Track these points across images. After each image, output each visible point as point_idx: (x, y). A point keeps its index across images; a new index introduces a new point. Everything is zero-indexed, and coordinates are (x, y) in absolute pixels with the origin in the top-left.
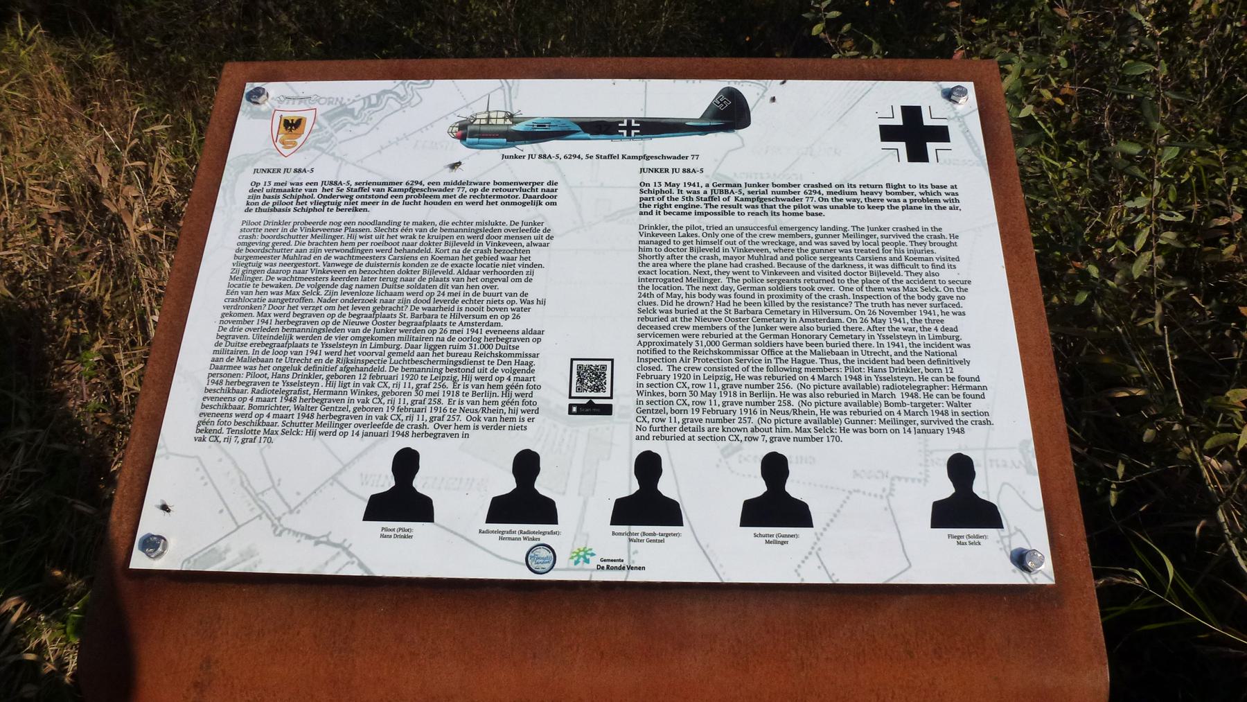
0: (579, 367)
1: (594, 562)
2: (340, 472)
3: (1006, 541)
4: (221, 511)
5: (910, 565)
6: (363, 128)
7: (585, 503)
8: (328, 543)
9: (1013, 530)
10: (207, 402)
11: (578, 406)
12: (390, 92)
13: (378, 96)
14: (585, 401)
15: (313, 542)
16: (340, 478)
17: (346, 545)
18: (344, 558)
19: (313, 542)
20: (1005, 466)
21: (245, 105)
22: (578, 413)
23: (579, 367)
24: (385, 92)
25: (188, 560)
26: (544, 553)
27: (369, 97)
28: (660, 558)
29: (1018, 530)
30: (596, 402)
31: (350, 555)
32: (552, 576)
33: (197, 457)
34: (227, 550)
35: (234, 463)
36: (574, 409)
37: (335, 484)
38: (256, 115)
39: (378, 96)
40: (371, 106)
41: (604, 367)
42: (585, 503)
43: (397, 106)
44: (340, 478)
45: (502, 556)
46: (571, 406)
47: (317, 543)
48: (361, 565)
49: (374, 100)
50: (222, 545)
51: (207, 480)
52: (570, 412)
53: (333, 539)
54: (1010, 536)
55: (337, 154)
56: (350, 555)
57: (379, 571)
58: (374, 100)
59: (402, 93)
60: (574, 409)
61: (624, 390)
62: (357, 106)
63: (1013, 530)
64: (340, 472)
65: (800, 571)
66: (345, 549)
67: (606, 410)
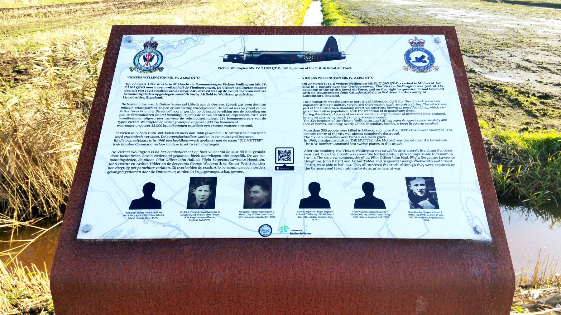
0: (280, 151)
1: (289, 231)
2: (174, 196)
3: (471, 221)
4: (118, 214)
5: (429, 232)
6: (179, 54)
7: (284, 207)
8: (169, 226)
9: (473, 217)
10: (111, 166)
11: (280, 167)
12: (190, 38)
13: (185, 40)
14: (282, 165)
15: (162, 225)
16: (174, 198)
17: (178, 226)
18: (177, 231)
19: (162, 225)
20: (468, 190)
21: (123, 44)
22: (280, 170)
23: (280, 151)
24: (188, 38)
25: (103, 235)
26: (266, 228)
27: (181, 40)
28: (318, 226)
29: (476, 217)
30: (287, 165)
31: (179, 230)
32: (270, 237)
33: (107, 191)
34: (121, 231)
35: (124, 193)
36: (278, 168)
37: (172, 201)
38: (128, 47)
39: (185, 40)
40: (182, 44)
41: (290, 151)
42: (284, 207)
43: (194, 45)
44: (174, 198)
46: (276, 167)
47: (164, 226)
48: (185, 234)
49: (183, 42)
50: (119, 229)
51: (111, 201)
52: (276, 169)
53: (171, 224)
54: (472, 219)
55: (167, 64)
56: (179, 230)
57: (192, 236)
58: (183, 42)
59: (196, 39)
60: (278, 168)
61: (299, 161)
62: (175, 44)
63: (473, 217)
64: (174, 196)
65: (379, 233)
66: (177, 228)
67: (292, 168)
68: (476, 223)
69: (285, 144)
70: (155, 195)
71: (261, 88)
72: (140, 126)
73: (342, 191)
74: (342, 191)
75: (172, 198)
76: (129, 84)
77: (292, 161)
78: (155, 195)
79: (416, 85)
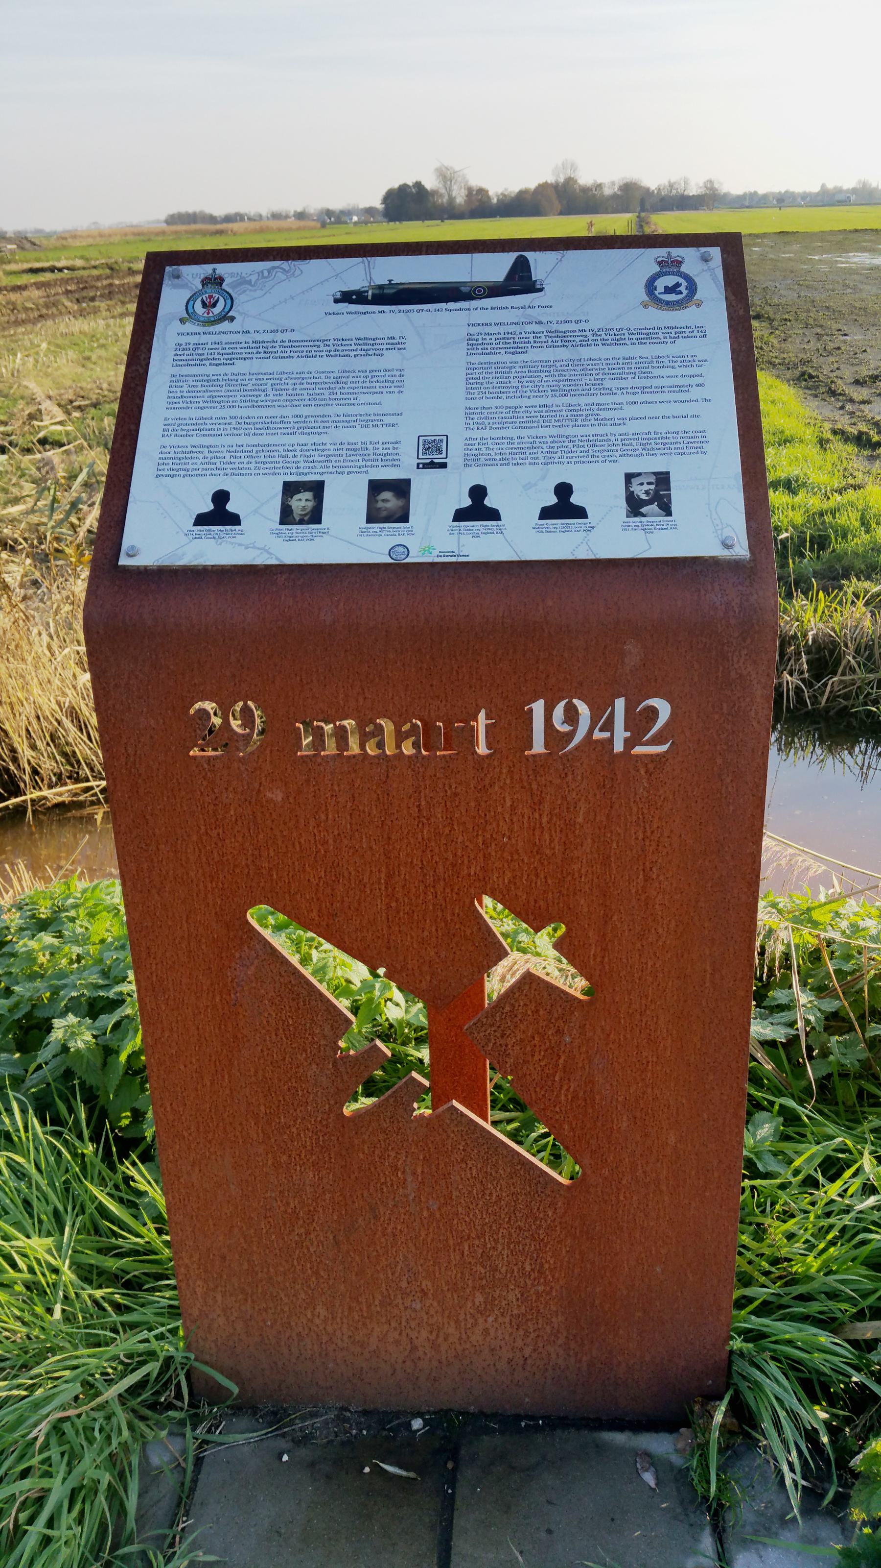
1: (436, 553)
6: (259, 293)
8: (254, 547)
10: (161, 467)
13: (269, 271)
18: (266, 555)
24: (274, 268)
26: (401, 549)
27: (262, 272)
28: (481, 545)
32: (408, 560)
39: (269, 271)
40: (263, 277)
43: (284, 277)
45: (374, 547)
49: (266, 273)
57: (289, 561)
58: (266, 273)
59: (287, 268)
61: (455, 455)
62: (254, 278)
66: (267, 551)
68: (727, 532)
69: (432, 429)
70: (230, 507)
71: (396, 344)
72: (202, 408)
73: (520, 496)
74: (520, 496)
75: (256, 511)
76: (180, 345)
77: (444, 455)
78: (230, 507)
79: (660, 331)
